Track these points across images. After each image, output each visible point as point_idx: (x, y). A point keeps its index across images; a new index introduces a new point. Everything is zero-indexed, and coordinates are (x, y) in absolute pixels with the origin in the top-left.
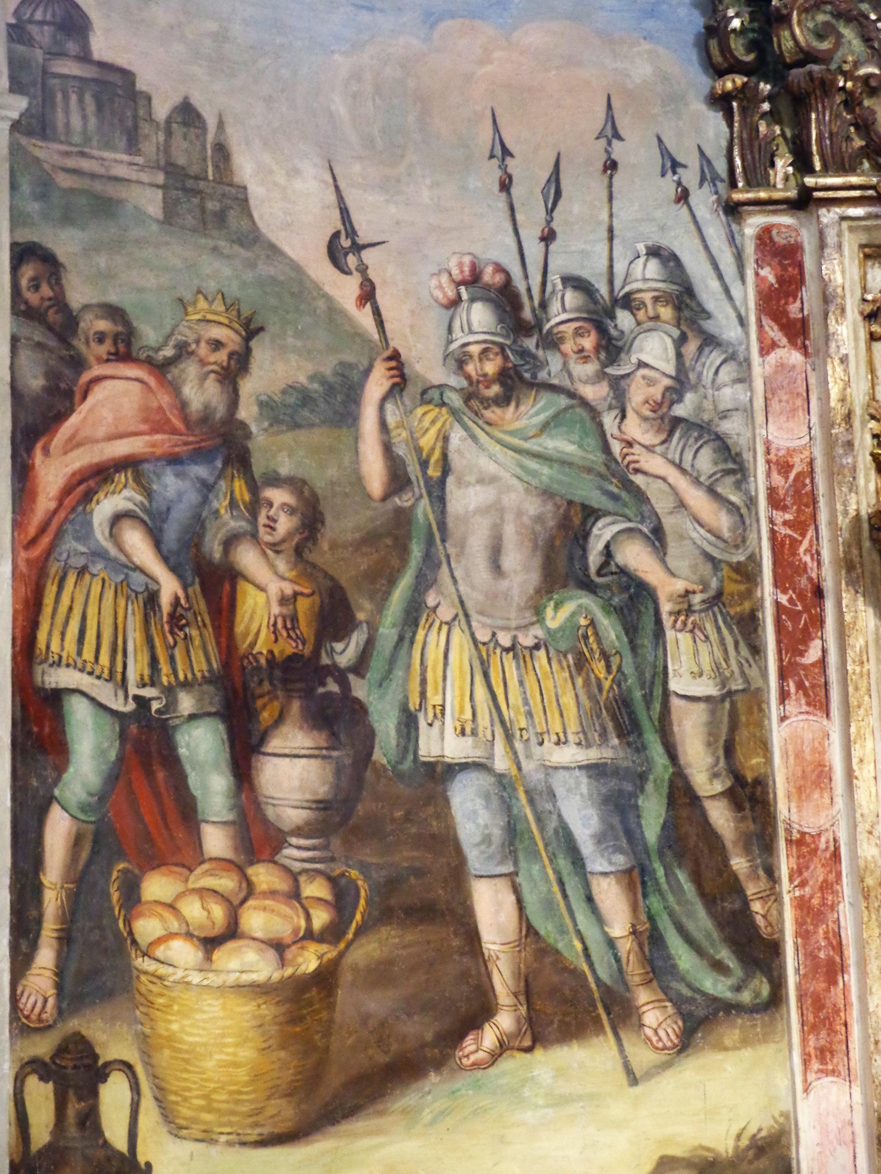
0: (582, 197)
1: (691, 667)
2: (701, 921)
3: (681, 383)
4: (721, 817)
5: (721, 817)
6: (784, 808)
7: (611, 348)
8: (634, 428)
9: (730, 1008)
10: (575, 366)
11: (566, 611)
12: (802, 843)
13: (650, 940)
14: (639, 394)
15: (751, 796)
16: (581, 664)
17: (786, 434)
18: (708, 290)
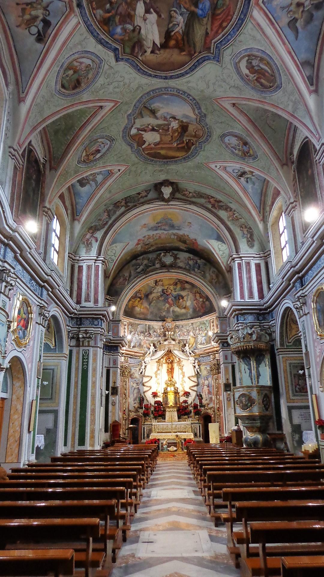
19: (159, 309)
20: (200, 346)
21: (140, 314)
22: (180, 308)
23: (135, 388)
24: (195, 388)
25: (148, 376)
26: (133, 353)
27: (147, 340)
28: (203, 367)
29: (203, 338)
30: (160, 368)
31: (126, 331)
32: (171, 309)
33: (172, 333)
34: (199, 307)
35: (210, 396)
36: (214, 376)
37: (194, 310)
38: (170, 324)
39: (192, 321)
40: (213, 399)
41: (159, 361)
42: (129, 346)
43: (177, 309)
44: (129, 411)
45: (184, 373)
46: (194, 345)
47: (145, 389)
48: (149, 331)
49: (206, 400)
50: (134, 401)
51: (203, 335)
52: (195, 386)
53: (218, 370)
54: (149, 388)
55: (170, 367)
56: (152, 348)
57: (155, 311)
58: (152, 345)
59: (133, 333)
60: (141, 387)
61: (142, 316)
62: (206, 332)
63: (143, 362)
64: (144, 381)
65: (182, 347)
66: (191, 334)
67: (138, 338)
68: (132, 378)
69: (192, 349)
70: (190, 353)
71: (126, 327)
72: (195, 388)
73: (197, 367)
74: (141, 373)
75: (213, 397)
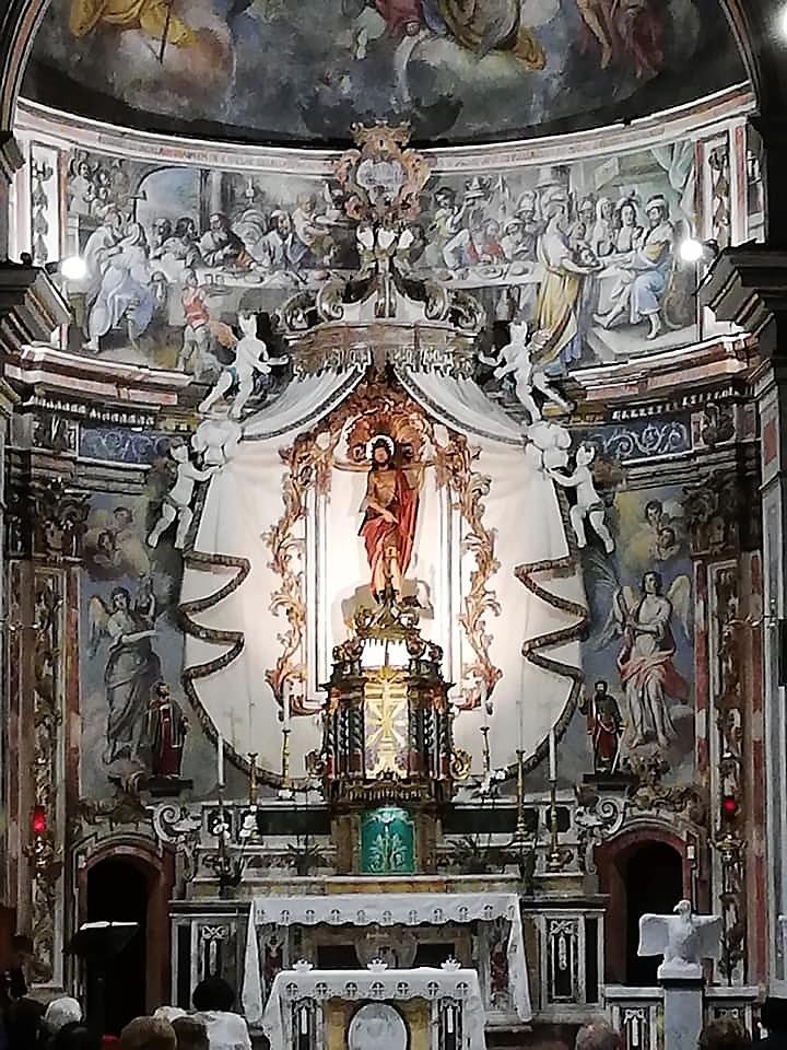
19: (308, 54)
20: (615, 343)
21: (156, 86)
22: (466, 44)
25: (219, 561)
26: (110, 389)
27: (213, 290)
28: (629, 502)
29: (644, 281)
30: (309, 498)
31: (51, 215)
32: (403, 54)
33: (407, 238)
34: (615, 39)
35: (678, 710)
37: (582, 63)
38: (388, 169)
39: (558, 149)
40: (700, 732)
42: (77, 337)
43: (444, 54)
44: (76, 808)
45: (490, 538)
47: (199, 652)
48: (226, 223)
49: (649, 738)
50: (113, 736)
51: (645, 256)
52: (563, 637)
54: (225, 649)
56: (251, 353)
57: (279, 66)
58: (249, 325)
59: (103, 233)
60: (161, 635)
61: (166, 110)
62: (662, 233)
63: (180, 453)
64: (183, 600)
65: (480, 345)
67: (141, 276)
68: (98, 573)
69: (554, 364)
70: (539, 397)
71: (50, 187)
72: (569, 654)
73: (588, 495)
75: (700, 717)
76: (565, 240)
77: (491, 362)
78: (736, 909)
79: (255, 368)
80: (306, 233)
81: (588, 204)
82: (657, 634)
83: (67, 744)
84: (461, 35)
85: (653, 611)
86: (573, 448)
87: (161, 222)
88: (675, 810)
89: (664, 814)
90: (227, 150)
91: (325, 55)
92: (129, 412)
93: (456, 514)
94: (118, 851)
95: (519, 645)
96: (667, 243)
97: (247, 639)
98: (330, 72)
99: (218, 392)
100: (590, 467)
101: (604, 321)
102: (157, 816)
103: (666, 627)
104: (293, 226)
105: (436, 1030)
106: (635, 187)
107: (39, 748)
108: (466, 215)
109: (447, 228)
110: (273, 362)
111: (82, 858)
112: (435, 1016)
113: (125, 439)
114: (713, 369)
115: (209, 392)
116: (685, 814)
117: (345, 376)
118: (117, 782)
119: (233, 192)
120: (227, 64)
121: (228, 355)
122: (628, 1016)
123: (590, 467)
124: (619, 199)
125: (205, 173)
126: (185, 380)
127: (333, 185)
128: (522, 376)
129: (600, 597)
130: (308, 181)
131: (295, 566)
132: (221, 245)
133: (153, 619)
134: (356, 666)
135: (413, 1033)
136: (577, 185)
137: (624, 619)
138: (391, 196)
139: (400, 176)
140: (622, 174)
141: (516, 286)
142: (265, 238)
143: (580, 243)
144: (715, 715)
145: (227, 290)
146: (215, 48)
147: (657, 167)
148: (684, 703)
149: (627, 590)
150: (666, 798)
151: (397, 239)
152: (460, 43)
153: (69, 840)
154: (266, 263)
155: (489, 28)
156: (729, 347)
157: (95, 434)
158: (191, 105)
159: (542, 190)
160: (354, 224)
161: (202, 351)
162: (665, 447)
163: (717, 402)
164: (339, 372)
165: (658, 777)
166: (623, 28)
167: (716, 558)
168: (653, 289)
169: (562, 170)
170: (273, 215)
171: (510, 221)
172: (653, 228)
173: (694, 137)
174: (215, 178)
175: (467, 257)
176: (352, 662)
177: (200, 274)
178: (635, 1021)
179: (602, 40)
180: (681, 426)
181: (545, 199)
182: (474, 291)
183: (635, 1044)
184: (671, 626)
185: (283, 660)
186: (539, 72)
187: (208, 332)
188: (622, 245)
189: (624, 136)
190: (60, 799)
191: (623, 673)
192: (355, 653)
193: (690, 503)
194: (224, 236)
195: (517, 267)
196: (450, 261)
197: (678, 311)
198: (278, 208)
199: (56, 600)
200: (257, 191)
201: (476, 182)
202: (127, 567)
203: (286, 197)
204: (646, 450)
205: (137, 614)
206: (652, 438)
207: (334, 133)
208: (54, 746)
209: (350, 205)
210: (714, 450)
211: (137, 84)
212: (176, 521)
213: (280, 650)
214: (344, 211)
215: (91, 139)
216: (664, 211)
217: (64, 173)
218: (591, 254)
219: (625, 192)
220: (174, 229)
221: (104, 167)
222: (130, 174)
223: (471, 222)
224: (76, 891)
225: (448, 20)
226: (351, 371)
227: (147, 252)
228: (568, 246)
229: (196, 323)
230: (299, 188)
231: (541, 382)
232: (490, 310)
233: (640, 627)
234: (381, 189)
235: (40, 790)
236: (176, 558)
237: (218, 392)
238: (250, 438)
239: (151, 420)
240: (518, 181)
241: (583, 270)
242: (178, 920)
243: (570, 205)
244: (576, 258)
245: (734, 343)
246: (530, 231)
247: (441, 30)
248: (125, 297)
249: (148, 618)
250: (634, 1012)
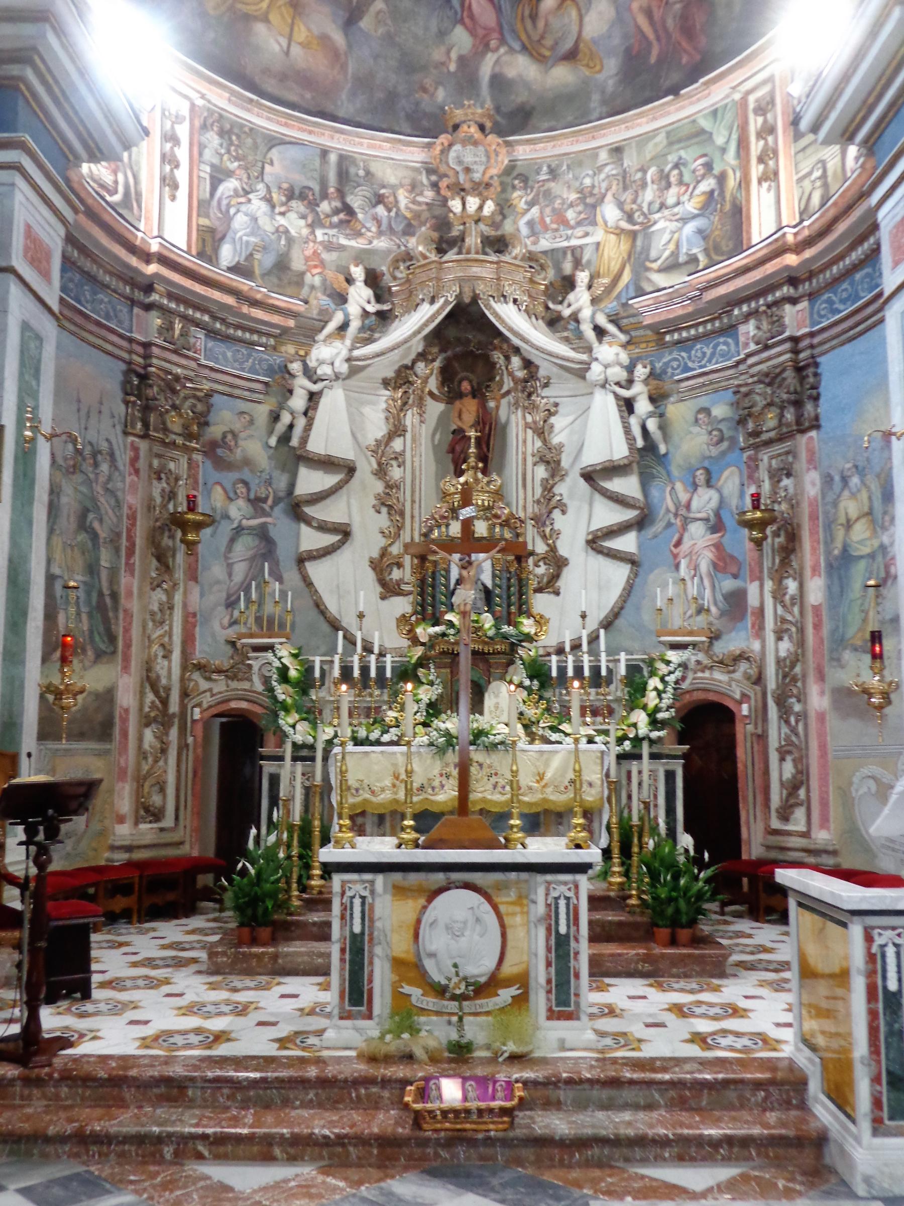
0: (93, 421)
1: (105, 558)
2: (101, 629)
3: (110, 479)
4: (108, 600)
5: (108, 600)
6: (122, 600)
7: (96, 465)
8: (99, 489)
9: (105, 653)
10: (87, 467)
11: (82, 537)
12: (125, 611)
13: (91, 632)
14: (102, 479)
15: (114, 596)
16: (83, 553)
17: (130, 499)
18: (117, 453)
19: (410, 66)
21: (283, 77)
22: (539, 58)
23: (239, 531)
24: (627, 543)
25: (327, 463)
26: (230, 300)
27: (330, 247)
28: (677, 410)
29: (690, 228)
31: (182, 154)
32: (487, 68)
33: (489, 208)
35: (728, 584)
36: (764, 457)
39: (617, 131)
40: (753, 600)
41: (401, 379)
43: (521, 67)
46: (626, 277)
47: (311, 539)
51: (691, 206)
53: (798, 404)
54: (333, 539)
55: (469, 417)
56: (360, 297)
58: (358, 272)
61: (292, 97)
65: (546, 293)
66: (610, 213)
68: (221, 464)
69: (611, 305)
70: (600, 332)
71: (183, 131)
72: (627, 543)
73: (643, 406)
74: (285, 438)
75: (753, 590)
76: (620, 205)
77: (559, 308)
78: (794, 760)
79: (364, 310)
80: (407, 208)
81: (639, 175)
82: (707, 520)
83: (185, 605)
84: (532, 50)
85: (704, 501)
86: (630, 369)
87: (285, 186)
88: (729, 672)
89: (719, 676)
90: (342, 132)
91: (424, 68)
92: (252, 331)
93: (529, 432)
94: (234, 705)
95: (582, 537)
96: (712, 192)
97: (356, 530)
98: (428, 82)
99: (331, 326)
100: (646, 382)
101: (655, 266)
102: (256, 668)
103: (718, 515)
104: (397, 201)
105: (542, 932)
106: (682, 153)
107: (155, 607)
108: (537, 195)
109: (522, 205)
110: (379, 307)
111: (197, 710)
112: (541, 909)
113: (250, 355)
114: (770, 268)
115: (323, 328)
116: (738, 675)
117: (437, 306)
118: (233, 644)
119: (347, 173)
120: (344, 67)
121: (342, 299)
122: (879, 941)
123: (646, 382)
124: (667, 163)
125: (324, 153)
126: (297, 305)
127: (430, 171)
128: (586, 313)
129: (655, 493)
130: (407, 167)
131: (396, 473)
132: (336, 212)
133: (272, 508)
134: (443, 529)
135: (510, 936)
136: (630, 161)
137: (677, 509)
138: (477, 176)
139: (484, 159)
140: (671, 144)
141: (581, 247)
142: (374, 211)
143: (634, 207)
144: (769, 585)
145: (342, 248)
146: (335, 55)
147: (702, 131)
148: (735, 576)
149: (679, 486)
150: (721, 662)
151: (481, 208)
152: (531, 55)
153: (185, 694)
154: (374, 229)
155: (556, 43)
156: (790, 239)
157: (219, 348)
158: (313, 98)
159: (600, 169)
160: (445, 201)
161: (319, 295)
162: (714, 357)
163: (769, 306)
164: (432, 301)
165: (711, 644)
166: (670, 23)
167: (769, 443)
168: (700, 231)
169: (617, 151)
170: (382, 191)
171: (573, 196)
172: (698, 182)
173: (737, 96)
174: (333, 158)
175: (538, 227)
176: (439, 526)
177: (319, 234)
178: (890, 951)
179: (651, 36)
180: (730, 340)
181: (602, 176)
182: (545, 253)
183: (893, 986)
184: (722, 512)
185: (384, 552)
186: (598, 76)
187: (324, 281)
188: (671, 201)
189: (672, 108)
190: (176, 656)
191: (675, 556)
192: (443, 517)
193: (742, 396)
194: (337, 204)
195: (579, 231)
196: (524, 231)
197: (723, 243)
198: (384, 187)
199: (177, 479)
200: (368, 173)
201: (545, 168)
202: (247, 462)
203: (393, 180)
204: (696, 365)
205: (256, 503)
206: (699, 354)
207: (430, 125)
208: (171, 608)
209: (443, 184)
210: (767, 347)
211: (266, 71)
212: (291, 426)
213: (383, 542)
214: (438, 192)
215: (221, 96)
216: (709, 166)
217: (197, 124)
218: (644, 214)
219: (672, 158)
220: (297, 192)
221: (236, 130)
222: (259, 141)
223: (541, 200)
224: (190, 740)
225: (524, 37)
226: (442, 300)
227: (273, 207)
228: (622, 209)
229: (315, 271)
230: (401, 173)
231: (602, 320)
232: (558, 267)
233: (692, 515)
234: (468, 170)
235: (155, 647)
236: (293, 455)
237: (331, 326)
238: (358, 359)
239: (272, 341)
240: (580, 164)
241: (637, 227)
242: (269, 768)
243: (624, 178)
244: (630, 218)
245: (795, 234)
246: (590, 203)
247: (517, 46)
248: (252, 239)
249: (266, 507)
250: (889, 933)
